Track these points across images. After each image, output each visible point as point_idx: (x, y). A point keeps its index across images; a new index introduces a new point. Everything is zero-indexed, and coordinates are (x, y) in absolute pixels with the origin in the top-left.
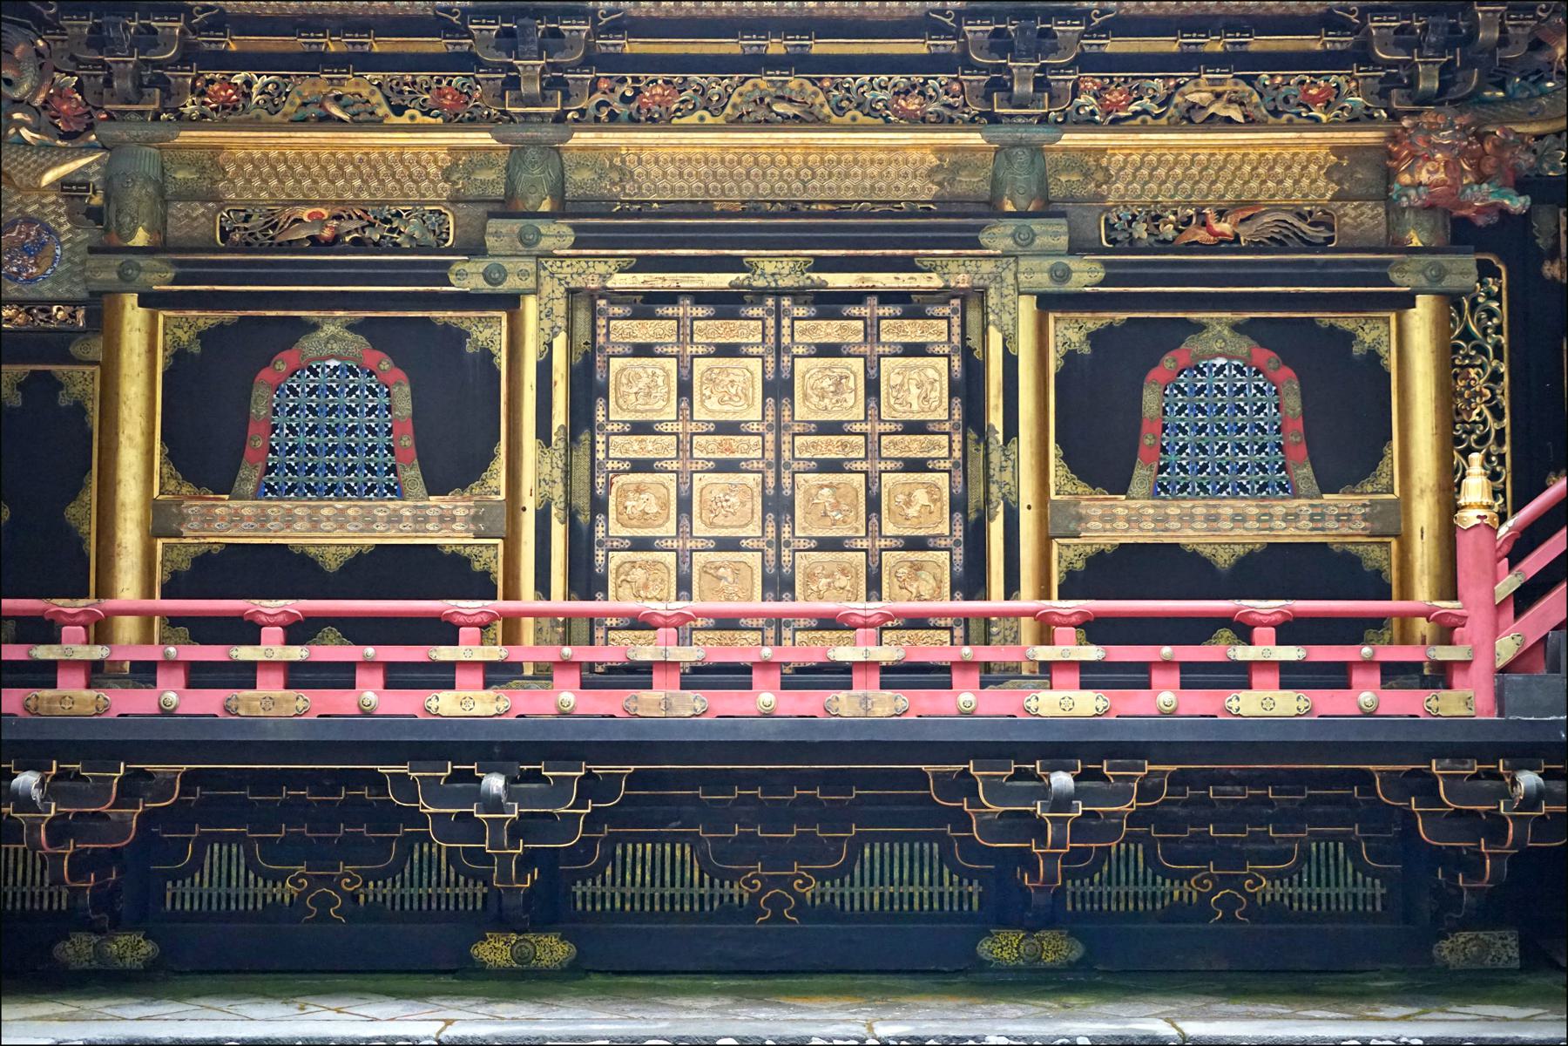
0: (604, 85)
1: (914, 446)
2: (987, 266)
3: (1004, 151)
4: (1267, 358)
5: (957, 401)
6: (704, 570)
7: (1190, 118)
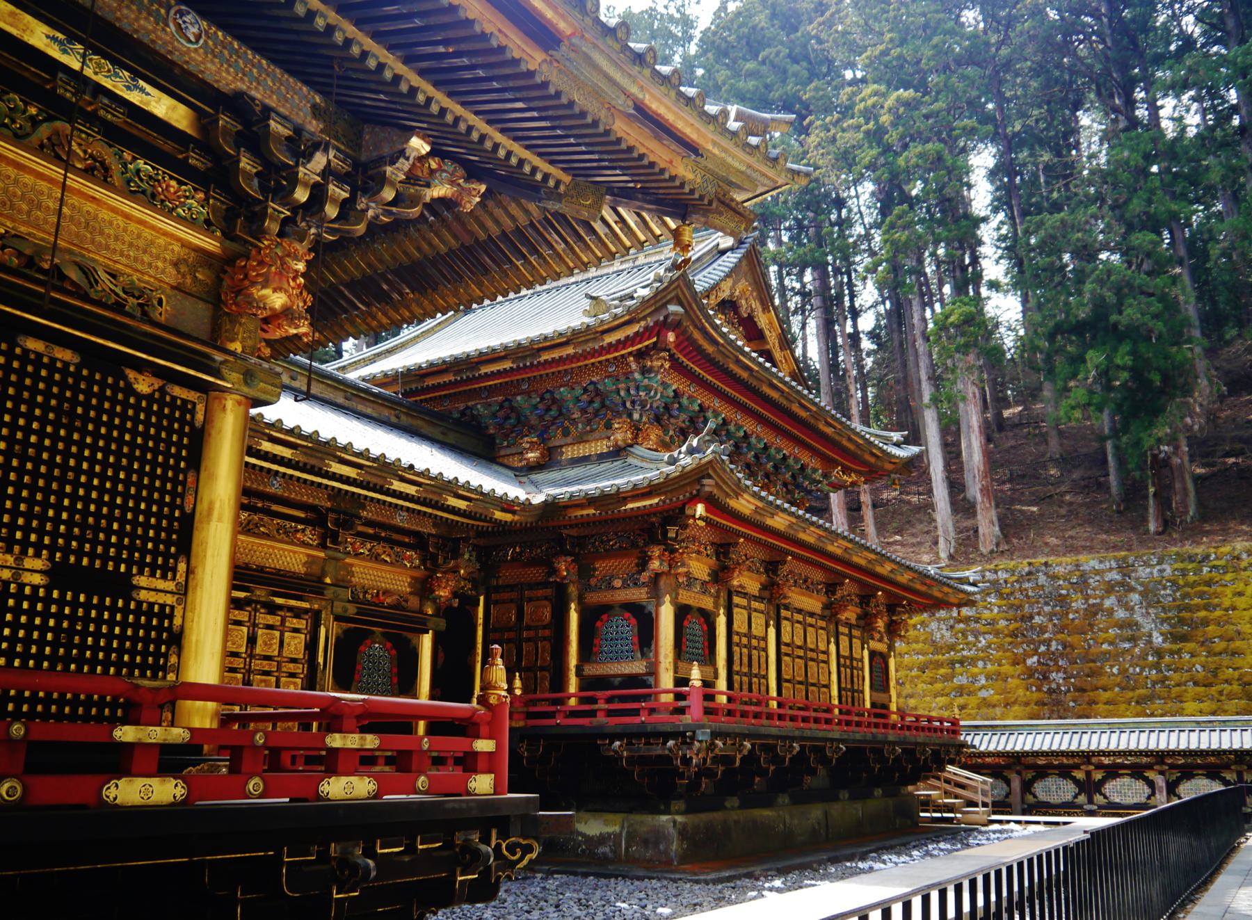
2: (324, 603)
4: (389, 645)
7: (376, 558)
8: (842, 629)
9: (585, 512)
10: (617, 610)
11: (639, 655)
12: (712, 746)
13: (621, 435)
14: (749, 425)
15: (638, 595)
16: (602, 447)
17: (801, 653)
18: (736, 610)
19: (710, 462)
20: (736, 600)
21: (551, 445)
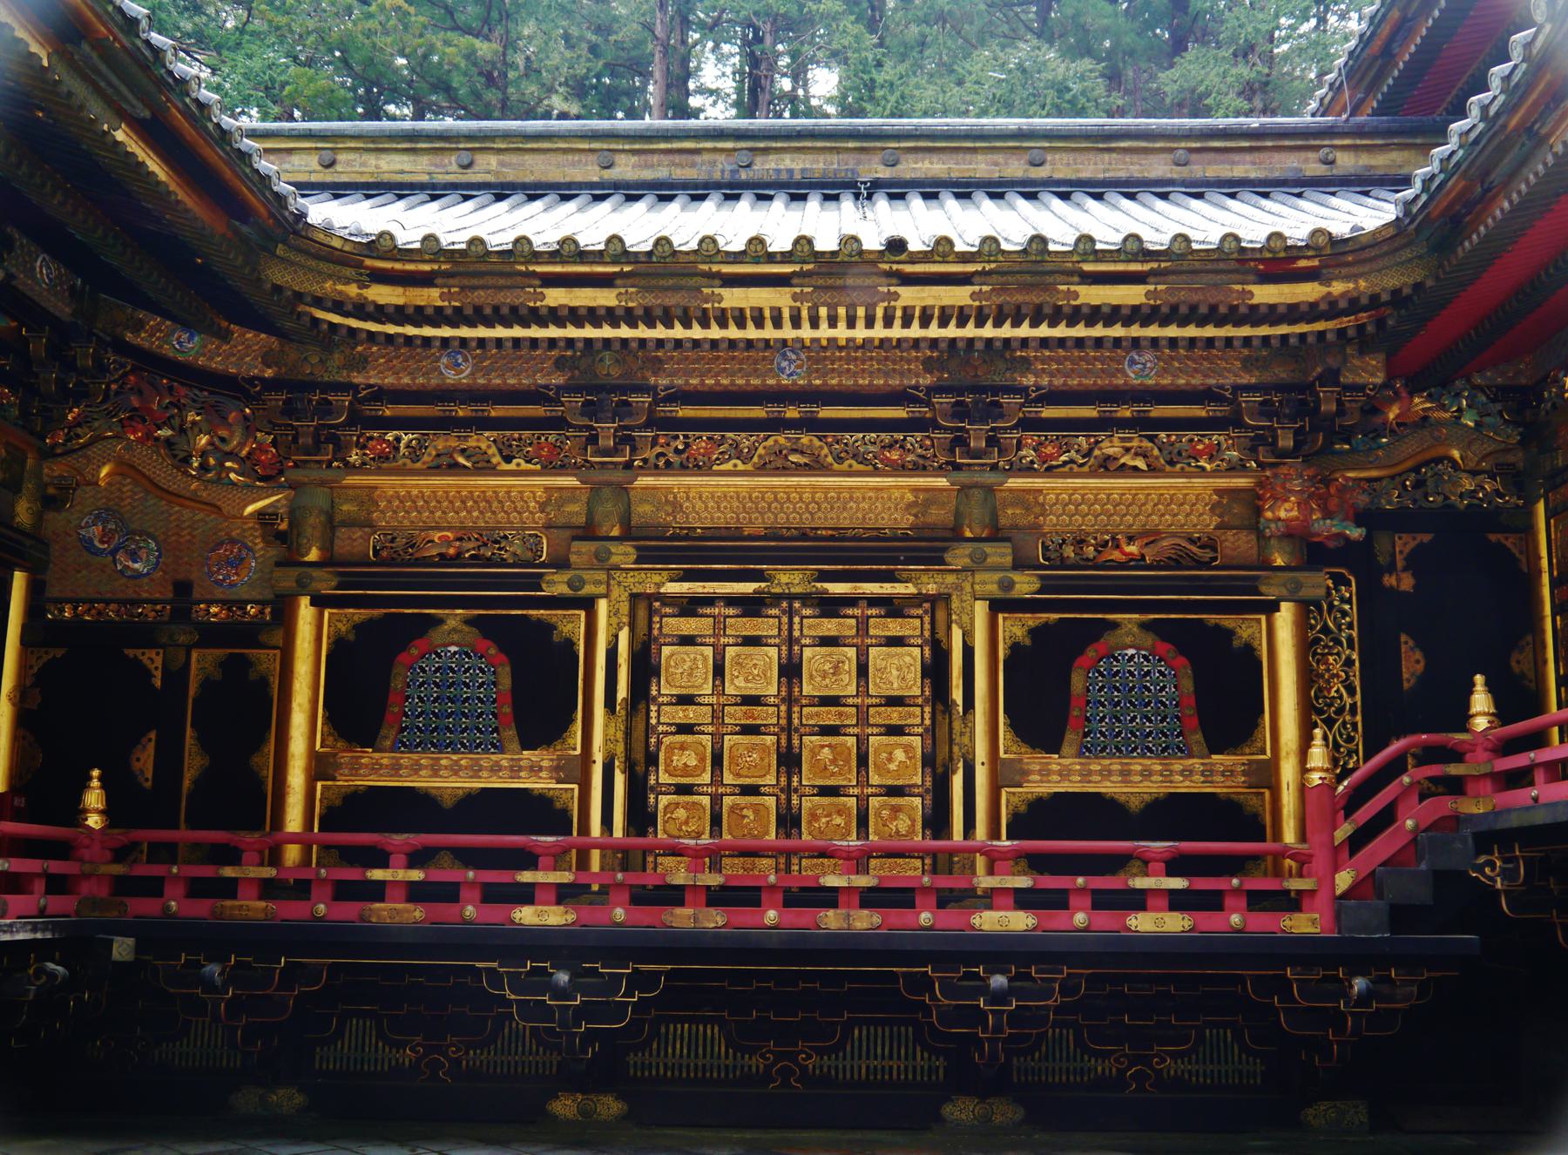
0: (662, 441)
1: (894, 716)
2: (950, 579)
3: (964, 489)
4: (1169, 650)
5: (927, 681)
6: (733, 809)
7: (1107, 466)
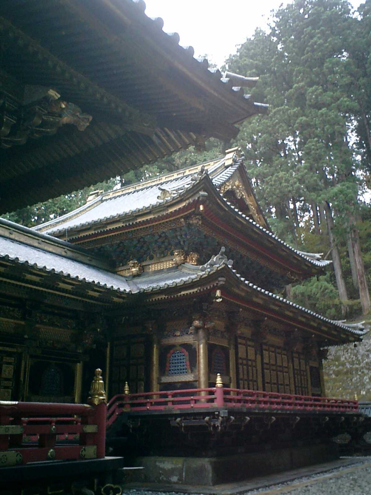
7: (52, 324)
8: (295, 355)
9: (160, 297)
10: (179, 348)
11: (190, 371)
12: (228, 419)
13: (178, 259)
14: (243, 252)
15: (189, 339)
16: (169, 264)
17: (274, 368)
18: (239, 346)
19: (223, 268)
20: (239, 340)
21: (144, 264)
